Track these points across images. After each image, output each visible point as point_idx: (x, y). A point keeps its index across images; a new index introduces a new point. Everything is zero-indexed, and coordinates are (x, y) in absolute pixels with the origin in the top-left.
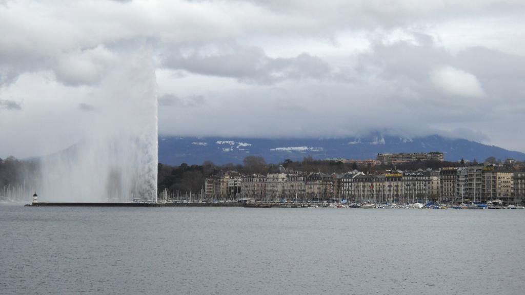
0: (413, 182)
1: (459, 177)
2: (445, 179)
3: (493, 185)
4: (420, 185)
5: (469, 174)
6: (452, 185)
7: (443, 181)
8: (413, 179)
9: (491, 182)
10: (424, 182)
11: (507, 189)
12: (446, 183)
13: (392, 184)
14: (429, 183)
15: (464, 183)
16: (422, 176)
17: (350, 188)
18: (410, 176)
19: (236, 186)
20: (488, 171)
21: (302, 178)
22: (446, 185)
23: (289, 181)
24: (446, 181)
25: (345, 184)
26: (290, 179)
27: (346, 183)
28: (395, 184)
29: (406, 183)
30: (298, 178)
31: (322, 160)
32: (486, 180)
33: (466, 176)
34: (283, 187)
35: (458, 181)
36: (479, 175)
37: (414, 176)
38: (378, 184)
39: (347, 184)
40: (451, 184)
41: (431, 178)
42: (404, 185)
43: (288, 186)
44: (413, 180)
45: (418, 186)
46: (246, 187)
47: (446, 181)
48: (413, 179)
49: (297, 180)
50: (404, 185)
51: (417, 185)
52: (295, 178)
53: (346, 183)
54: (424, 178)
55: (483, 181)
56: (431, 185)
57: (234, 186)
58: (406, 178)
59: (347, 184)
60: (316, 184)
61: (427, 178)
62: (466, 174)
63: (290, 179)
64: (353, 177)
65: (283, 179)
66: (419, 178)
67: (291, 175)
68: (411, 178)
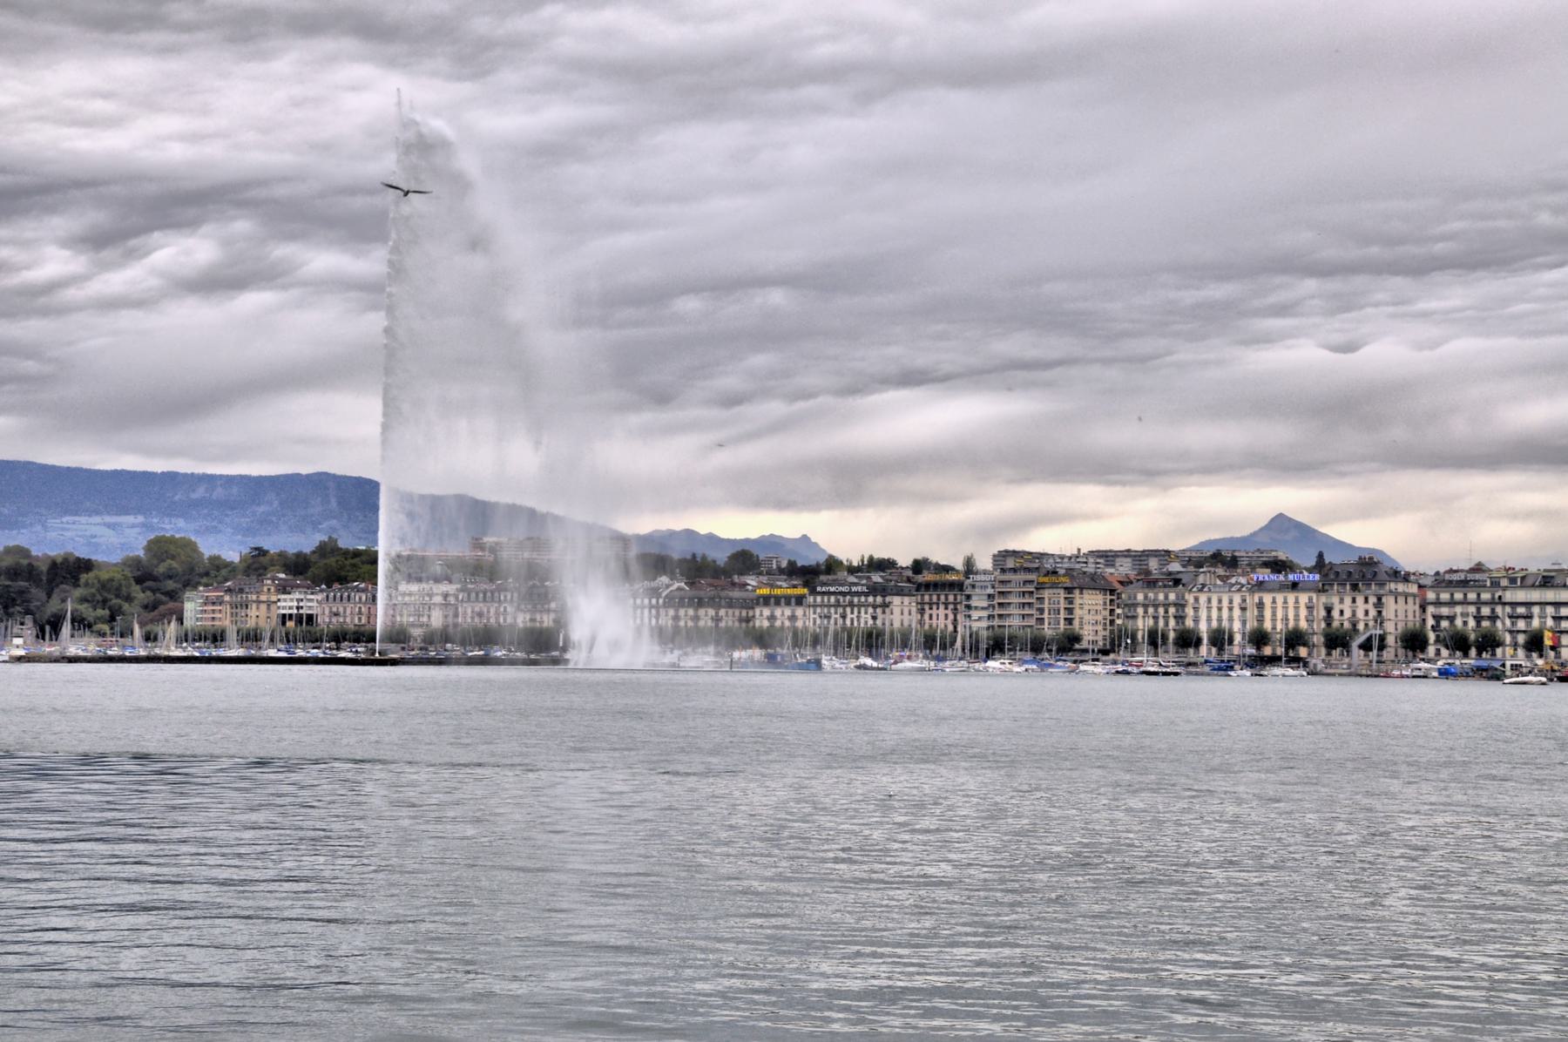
0: (840, 610)
1: (969, 597)
2: (931, 604)
3: (1065, 619)
4: (858, 617)
5: (999, 592)
6: (951, 617)
7: (927, 607)
8: (838, 601)
9: (1062, 611)
10: (870, 610)
11: (1095, 628)
12: (934, 612)
13: (778, 612)
14: (884, 612)
15: (985, 614)
16: (866, 595)
18: (830, 593)
19: (301, 611)
20: (1054, 586)
21: (509, 597)
22: (934, 617)
23: (469, 600)
24: (935, 607)
26: (473, 595)
28: (788, 612)
29: (819, 610)
30: (496, 594)
31: (351, 548)
32: (1046, 606)
33: (990, 596)
34: (446, 617)
35: (968, 607)
36: (1027, 596)
37: (844, 594)
38: (730, 611)
40: (946, 616)
41: (888, 599)
42: (812, 616)
43: (465, 613)
44: (837, 605)
45: (852, 620)
46: (336, 614)
47: (935, 607)
48: (838, 601)
49: (493, 600)
50: (812, 616)
51: (849, 616)
52: (489, 594)
54: (871, 599)
55: (1038, 609)
56: (888, 616)
57: (295, 611)
58: (819, 599)
60: (548, 611)
61: (879, 599)
62: (990, 591)
63: (473, 595)
64: (664, 595)
65: (446, 596)
66: (856, 600)
67: (472, 586)
68: (833, 599)
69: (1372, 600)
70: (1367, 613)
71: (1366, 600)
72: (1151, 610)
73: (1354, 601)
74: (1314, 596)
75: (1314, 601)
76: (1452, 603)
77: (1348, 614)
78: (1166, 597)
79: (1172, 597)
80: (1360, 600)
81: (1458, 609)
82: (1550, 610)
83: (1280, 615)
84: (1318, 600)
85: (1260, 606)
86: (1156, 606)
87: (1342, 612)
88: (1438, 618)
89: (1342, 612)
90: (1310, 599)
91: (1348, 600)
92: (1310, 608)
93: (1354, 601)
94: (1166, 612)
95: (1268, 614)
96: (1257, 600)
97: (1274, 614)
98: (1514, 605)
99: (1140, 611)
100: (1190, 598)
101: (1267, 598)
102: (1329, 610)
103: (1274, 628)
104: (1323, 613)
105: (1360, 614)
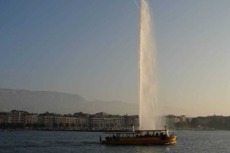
71: (85, 119)
72: (48, 120)
77: (82, 121)
80: (84, 119)
83: (71, 121)
85: (68, 119)
86: (49, 119)
87: (81, 121)
88: (95, 122)
89: (81, 121)
91: (82, 119)
94: (51, 120)
95: (69, 120)
97: (70, 121)
98: (105, 120)
99: (46, 120)
101: (69, 118)
102: (79, 120)
103: (70, 123)
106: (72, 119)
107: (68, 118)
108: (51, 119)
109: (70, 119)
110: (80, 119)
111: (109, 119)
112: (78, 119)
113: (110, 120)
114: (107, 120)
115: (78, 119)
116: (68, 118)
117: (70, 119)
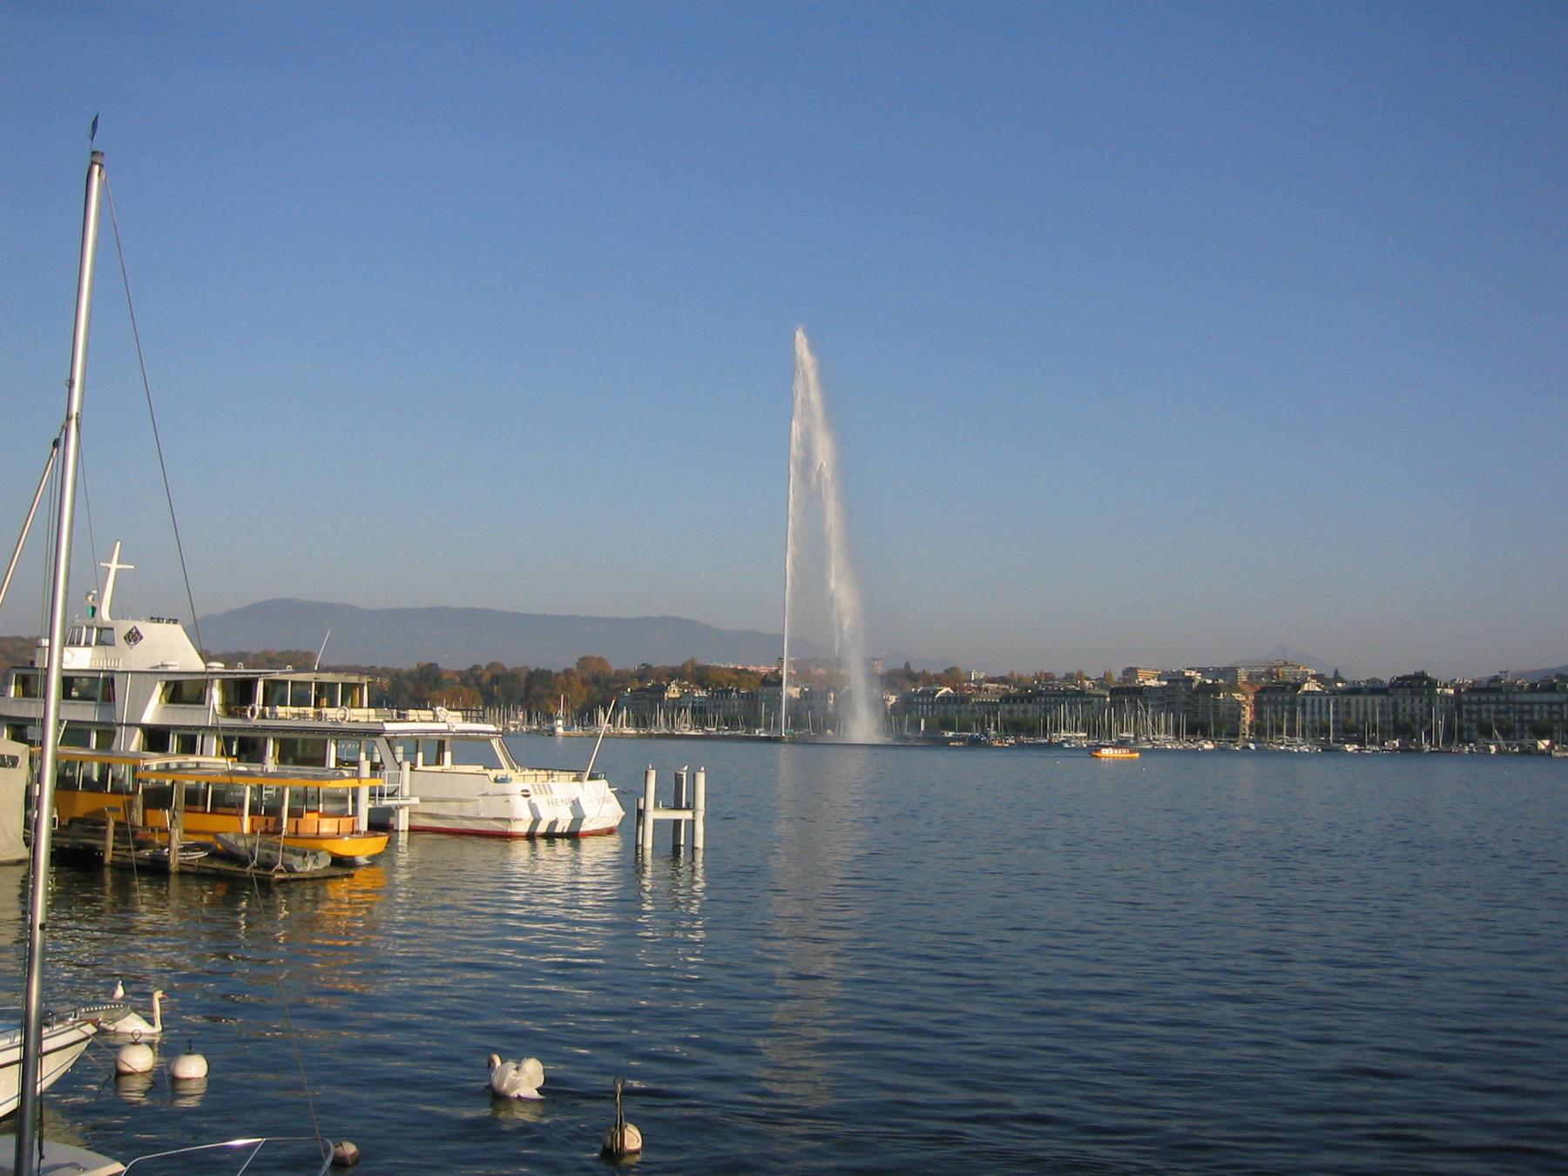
17: (930, 714)
25: (920, 707)
27: (923, 704)
28: (1022, 707)
39: (925, 707)
53: (923, 704)
59: (925, 707)
69: (1425, 700)
70: (1421, 710)
71: (1421, 701)
73: (1412, 701)
74: (1384, 697)
75: (1385, 701)
76: (1480, 702)
77: (1408, 710)
78: (1283, 699)
79: (1287, 698)
81: (1484, 707)
82: (1546, 707)
84: (1388, 700)
85: (1348, 704)
90: (1382, 700)
91: (1408, 701)
92: (1382, 705)
93: (1412, 701)
95: (1353, 709)
96: (1345, 701)
97: (1358, 711)
100: (1300, 699)
101: (1353, 699)
102: (1395, 705)
104: (1391, 709)
105: (1417, 710)
106: (1365, 702)
107: (1348, 700)
108: (1283, 703)
109: (1358, 702)
110: (1400, 701)
111: (1546, 697)
112: (1391, 700)
113: (1550, 704)
114: (1531, 704)
115: (1391, 700)
116: (1348, 700)
117: (1358, 702)
